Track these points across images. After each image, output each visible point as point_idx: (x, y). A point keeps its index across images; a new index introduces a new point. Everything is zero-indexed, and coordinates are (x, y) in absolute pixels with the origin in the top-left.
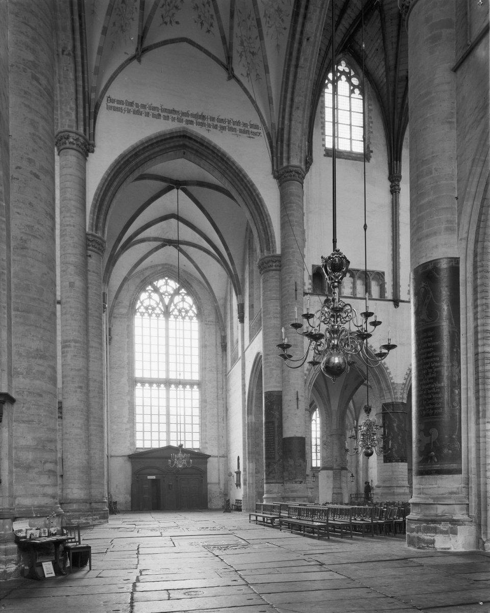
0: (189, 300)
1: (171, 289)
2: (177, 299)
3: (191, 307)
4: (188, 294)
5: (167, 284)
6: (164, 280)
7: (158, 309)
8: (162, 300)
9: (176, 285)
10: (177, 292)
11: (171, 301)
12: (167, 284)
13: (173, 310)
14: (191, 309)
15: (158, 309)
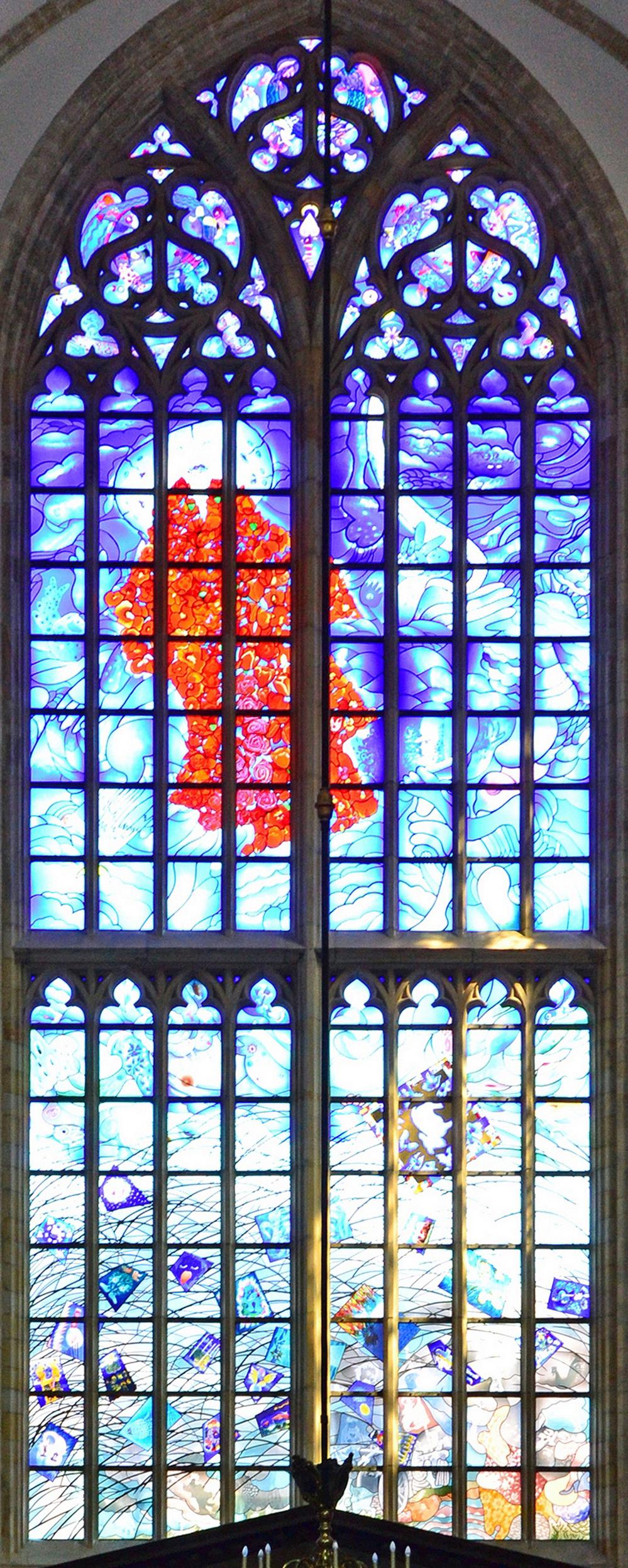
0: (512, 218)
1: (351, 134)
2: (413, 219)
3: (528, 278)
4: (496, 173)
5: (311, 96)
6: (289, 68)
7: (229, 322)
8: (267, 240)
9: (394, 99)
10: (399, 157)
11: (353, 237)
12: (311, 96)
13: (369, 324)
14: (529, 301)
15: (229, 322)
